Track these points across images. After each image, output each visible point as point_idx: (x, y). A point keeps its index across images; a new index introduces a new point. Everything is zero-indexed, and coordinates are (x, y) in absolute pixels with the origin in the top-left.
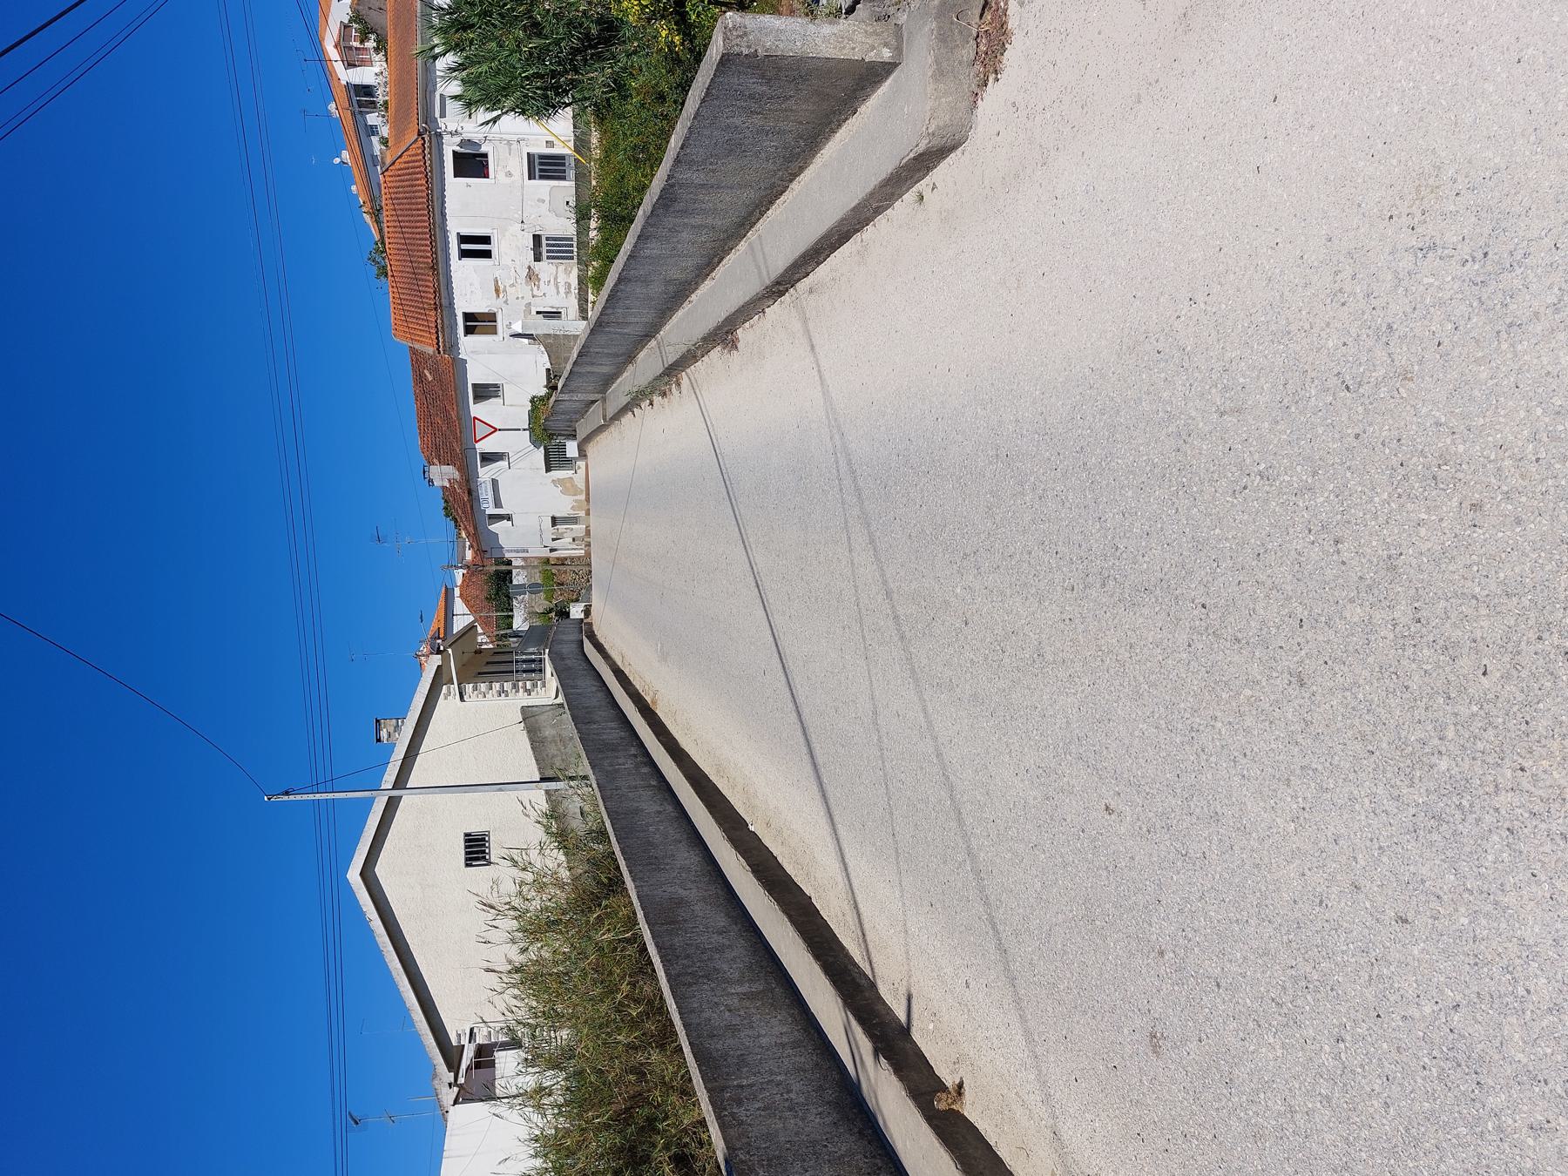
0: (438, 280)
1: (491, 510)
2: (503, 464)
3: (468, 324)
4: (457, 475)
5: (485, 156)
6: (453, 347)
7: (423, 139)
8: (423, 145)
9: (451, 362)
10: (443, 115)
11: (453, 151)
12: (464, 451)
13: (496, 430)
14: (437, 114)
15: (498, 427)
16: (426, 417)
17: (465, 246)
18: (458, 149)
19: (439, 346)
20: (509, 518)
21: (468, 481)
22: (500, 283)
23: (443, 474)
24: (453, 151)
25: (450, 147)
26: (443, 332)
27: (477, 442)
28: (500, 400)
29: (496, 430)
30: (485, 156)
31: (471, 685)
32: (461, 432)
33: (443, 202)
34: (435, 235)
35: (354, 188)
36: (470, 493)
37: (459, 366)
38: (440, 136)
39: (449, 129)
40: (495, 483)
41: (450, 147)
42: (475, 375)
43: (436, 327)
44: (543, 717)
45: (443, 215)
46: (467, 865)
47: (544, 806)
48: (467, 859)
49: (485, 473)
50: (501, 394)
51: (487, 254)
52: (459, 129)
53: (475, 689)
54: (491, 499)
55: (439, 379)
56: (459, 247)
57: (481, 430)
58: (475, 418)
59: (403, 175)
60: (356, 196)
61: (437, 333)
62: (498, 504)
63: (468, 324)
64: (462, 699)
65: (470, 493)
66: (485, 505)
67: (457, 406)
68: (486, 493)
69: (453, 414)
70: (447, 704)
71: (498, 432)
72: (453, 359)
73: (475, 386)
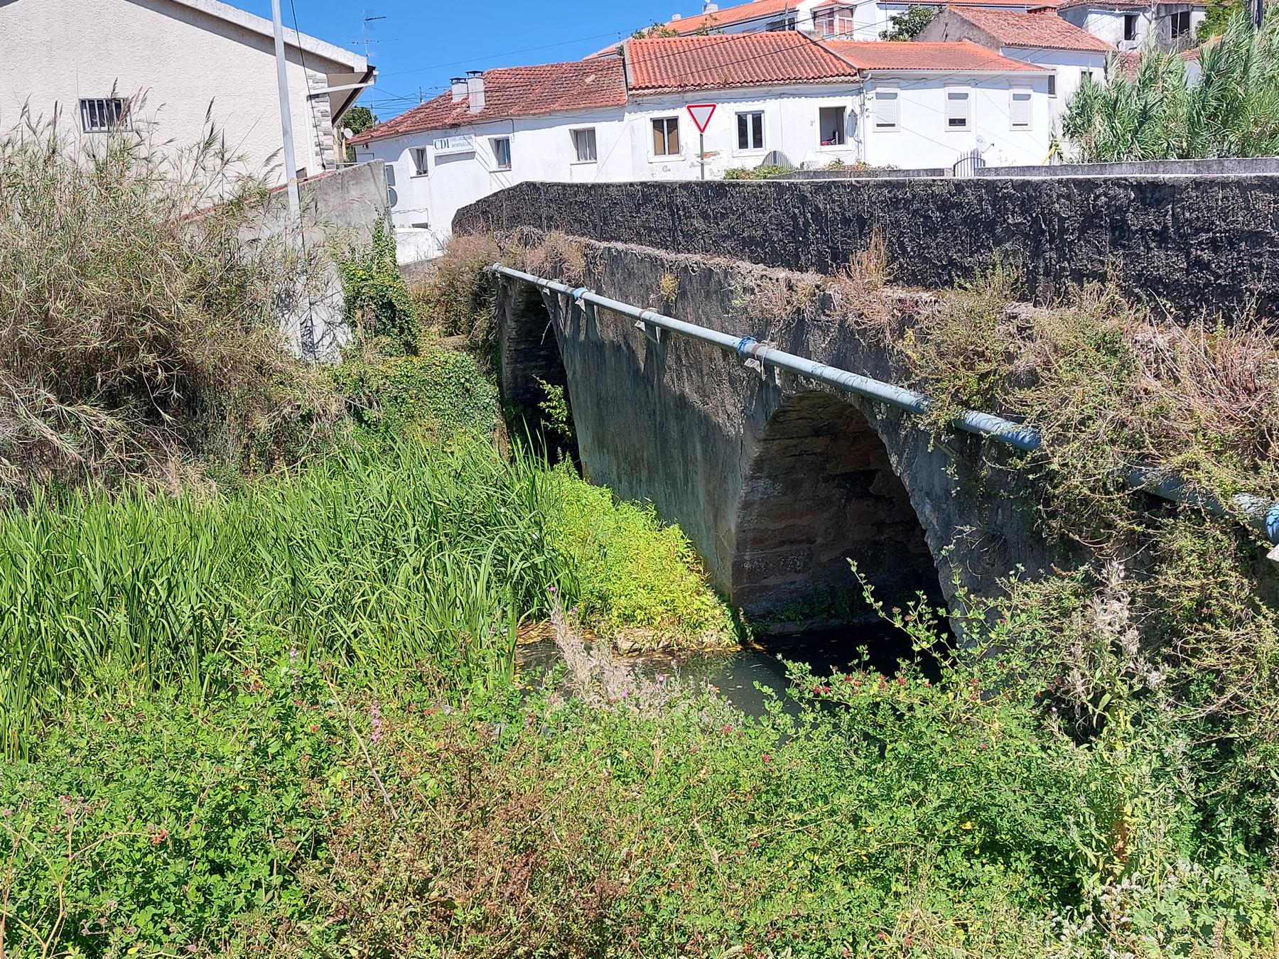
0: (713, 89)
1: (431, 152)
2: (493, 163)
3: (665, 123)
4: (474, 111)
5: (841, 141)
6: (638, 105)
7: (855, 74)
8: (849, 74)
9: (620, 103)
10: (879, 96)
11: (844, 108)
12: (509, 118)
13: (702, 131)
14: (879, 90)
15: (704, 134)
16: (531, 79)
17: (750, 119)
18: (848, 111)
19: (637, 89)
20: (422, 171)
21: (470, 123)
22: (713, 158)
23: (474, 95)
24: (844, 108)
25: (849, 103)
26: (655, 94)
27: (689, 107)
28: (575, 160)
29: (702, 131)
30: (841, 141)
31: (328, 109)
32: (534, 114)
33: (793, 95)
34: (742, 87)
35: (678, 17)
36: (454, 126)
37: (615, 110)
38: (859, 91)
39: (866, 101)
40: (471, 155)
41: (849, 103)
42: (605, 131)
43: (660, 86)
44: (373, 187)
45: (781, 95)
46: (83, 102)
47: (273, 183)
48: (91, 102)
49: (482, 144)
50: (582, 161)
51: (743, 144)
52: (867, 114)
53: (324, 114)
54: (446, 151)
55: (589, 92)
56: (749, 113)
57: (701, 113)
58: (714, 106)
59: (808, 55)
60: (669, 19)
61: (653, 87)
62: (440, 159)
63: (665, 123)
64: (311, 97)
65: (454, 126)
66: (439, 145)
67: (567, 110)
68: (456, 144)
69: (556, 106)
70: (320, 81)
71: (698, 132)
72: (623, 106)
73: (592, 131)
